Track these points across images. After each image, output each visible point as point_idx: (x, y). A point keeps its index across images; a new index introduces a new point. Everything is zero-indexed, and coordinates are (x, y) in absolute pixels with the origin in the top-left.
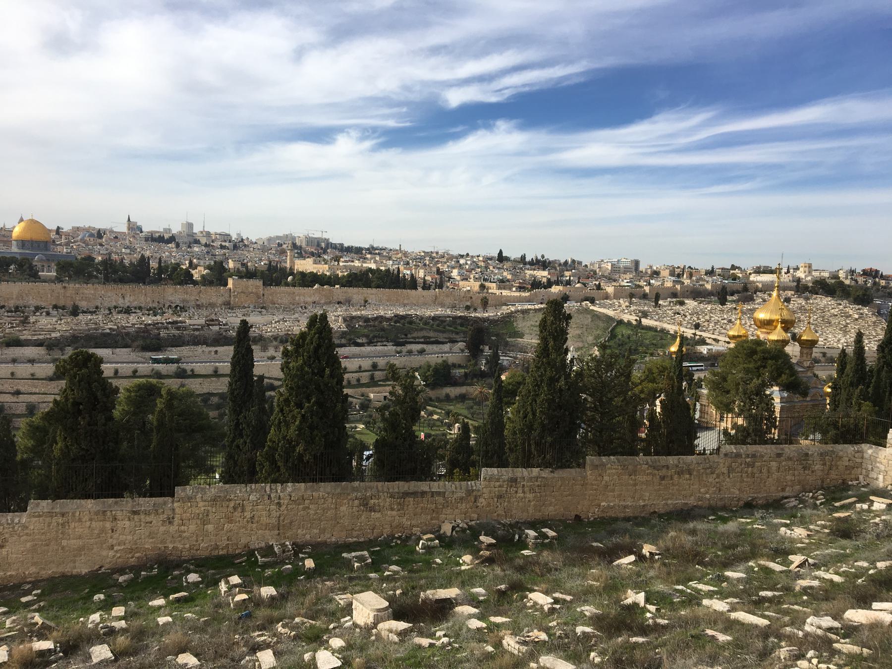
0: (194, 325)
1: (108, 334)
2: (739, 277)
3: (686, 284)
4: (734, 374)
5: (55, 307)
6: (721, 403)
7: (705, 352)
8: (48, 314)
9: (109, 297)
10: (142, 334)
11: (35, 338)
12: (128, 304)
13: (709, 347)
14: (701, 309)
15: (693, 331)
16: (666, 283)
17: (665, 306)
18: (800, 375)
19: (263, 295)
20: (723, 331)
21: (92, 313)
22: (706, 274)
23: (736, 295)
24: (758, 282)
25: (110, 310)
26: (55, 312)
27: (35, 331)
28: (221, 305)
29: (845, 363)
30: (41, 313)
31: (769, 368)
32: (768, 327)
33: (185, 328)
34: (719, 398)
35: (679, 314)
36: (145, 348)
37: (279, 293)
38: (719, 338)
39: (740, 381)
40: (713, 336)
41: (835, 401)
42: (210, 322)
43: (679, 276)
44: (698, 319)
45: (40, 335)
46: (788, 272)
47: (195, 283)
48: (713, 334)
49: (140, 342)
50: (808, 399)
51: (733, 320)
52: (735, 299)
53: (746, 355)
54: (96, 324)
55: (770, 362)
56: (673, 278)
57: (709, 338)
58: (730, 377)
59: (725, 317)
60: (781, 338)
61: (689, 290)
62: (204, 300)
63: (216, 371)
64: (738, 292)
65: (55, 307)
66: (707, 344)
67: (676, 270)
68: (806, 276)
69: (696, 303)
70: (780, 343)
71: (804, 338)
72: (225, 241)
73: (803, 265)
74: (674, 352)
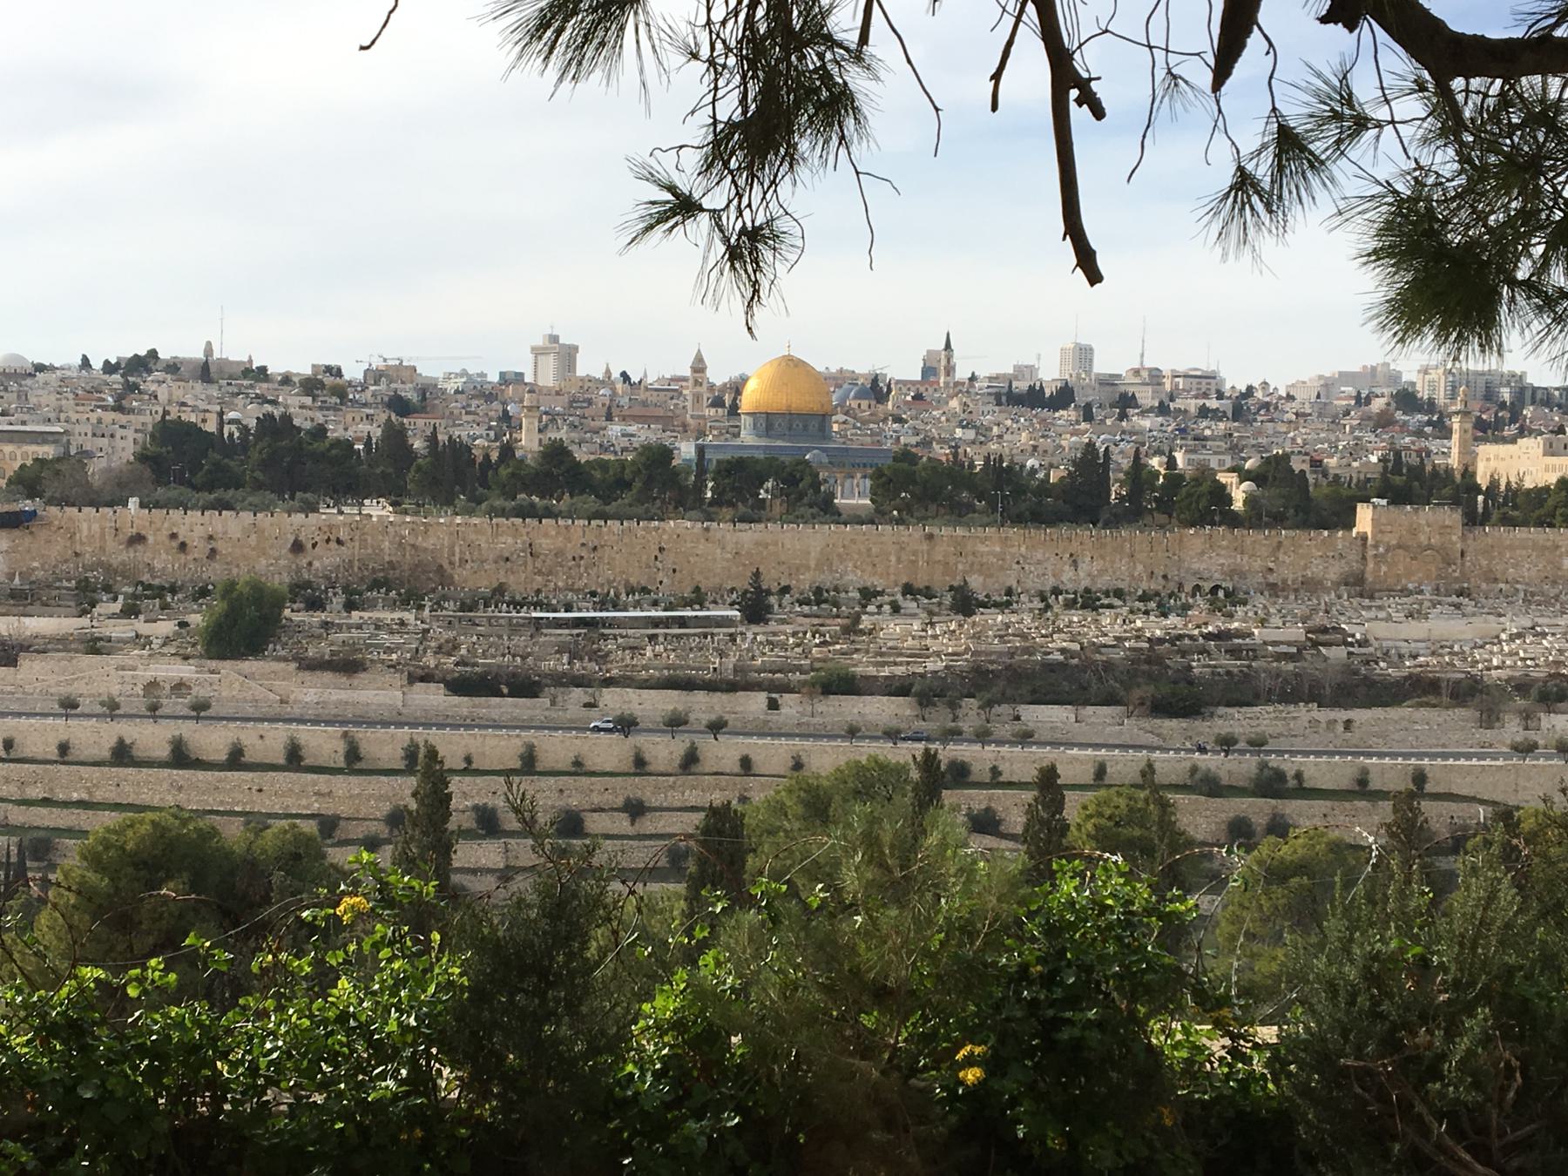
0: (1275, 643)
1: (1060, 664)
5: (908, 590)
8: (896, 609)
9: (1039, 562)
10: (1145, 667)
11: (886, 672)
12: (1086, 583)
19: (1462, 554)
21: (1002, 606)
25: (1043, 599)
26: (909, 605)
27: (882, 654)
28: (1337, 584)
30: (880, 607)
33: (1254, 653)
36: (1162, 708)
37: (1511, 548)
42: (1322, 635)
45: (895, 664)
47: (1233, 520)
49: (1145, 691)
54: (1024, 636)
62: (1288, 571)
63: (1363, 782)
65: (908, 590)
72: (1206, 395)
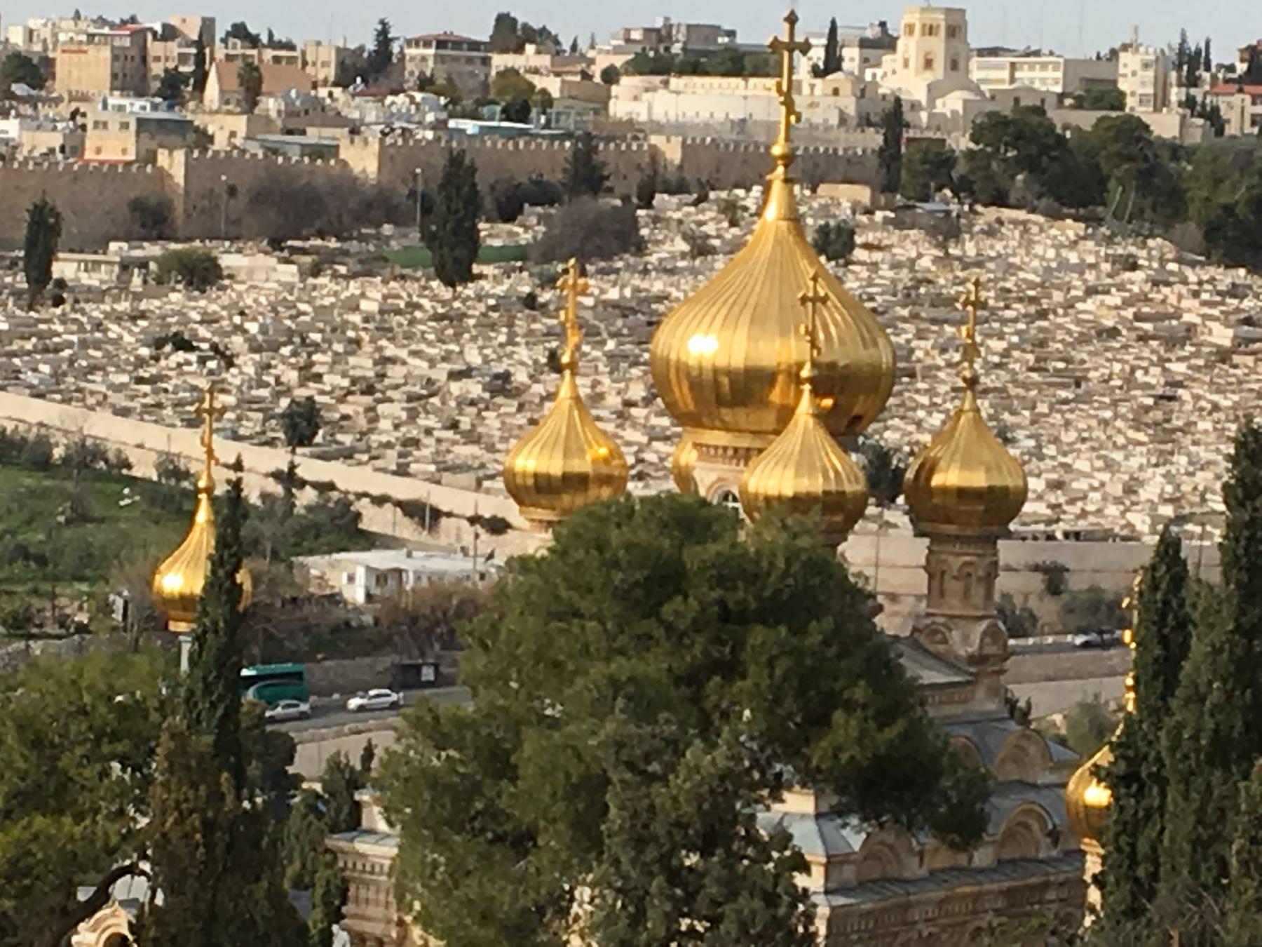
2: (547, 101)
3: (220, 143)
4: (554, 723)
6: (485, 918)
7: (356, 594)
13: (381, 559)
14: (321, 310)
15: (279, 458)
16: (92, 139)
17: (97, 295)
18: (932, 713)
20: (465, 452)
22: (343, 81)
23: (532, 214)
24: (659, 128)
29: (1183, 624)
31: (755, 677)
32: (740, 416)
34: (470, 888)
35: (183, 344)
38: (440, 497)
39: (608, 759)
40: (403, 489)
41: (1134, 862)
43: (172, 88)
44: (308, 374)
46: (832, 63)
48: (402, 471)
50: (982, 857)
51: (520, 376)
52: (525, 237)
53: (622, 595)
55: (758, 635)
56: (137, 106)
57: (380, 501)
58: (531, 744)
59: (473, 357)
60: (815, 485)
61: (245, 184)
64: (543, 194)
66: (370, 541)
67: (155, 48)
68: (935, 91)
69: (289, 273)
70: (815, 516)
71: (948, 477)
73: (916, 19)
74: (185, 602)
